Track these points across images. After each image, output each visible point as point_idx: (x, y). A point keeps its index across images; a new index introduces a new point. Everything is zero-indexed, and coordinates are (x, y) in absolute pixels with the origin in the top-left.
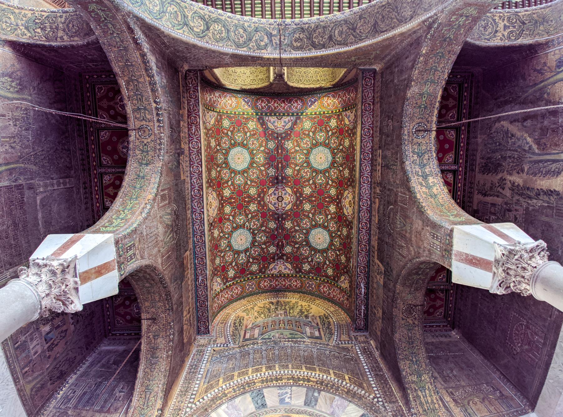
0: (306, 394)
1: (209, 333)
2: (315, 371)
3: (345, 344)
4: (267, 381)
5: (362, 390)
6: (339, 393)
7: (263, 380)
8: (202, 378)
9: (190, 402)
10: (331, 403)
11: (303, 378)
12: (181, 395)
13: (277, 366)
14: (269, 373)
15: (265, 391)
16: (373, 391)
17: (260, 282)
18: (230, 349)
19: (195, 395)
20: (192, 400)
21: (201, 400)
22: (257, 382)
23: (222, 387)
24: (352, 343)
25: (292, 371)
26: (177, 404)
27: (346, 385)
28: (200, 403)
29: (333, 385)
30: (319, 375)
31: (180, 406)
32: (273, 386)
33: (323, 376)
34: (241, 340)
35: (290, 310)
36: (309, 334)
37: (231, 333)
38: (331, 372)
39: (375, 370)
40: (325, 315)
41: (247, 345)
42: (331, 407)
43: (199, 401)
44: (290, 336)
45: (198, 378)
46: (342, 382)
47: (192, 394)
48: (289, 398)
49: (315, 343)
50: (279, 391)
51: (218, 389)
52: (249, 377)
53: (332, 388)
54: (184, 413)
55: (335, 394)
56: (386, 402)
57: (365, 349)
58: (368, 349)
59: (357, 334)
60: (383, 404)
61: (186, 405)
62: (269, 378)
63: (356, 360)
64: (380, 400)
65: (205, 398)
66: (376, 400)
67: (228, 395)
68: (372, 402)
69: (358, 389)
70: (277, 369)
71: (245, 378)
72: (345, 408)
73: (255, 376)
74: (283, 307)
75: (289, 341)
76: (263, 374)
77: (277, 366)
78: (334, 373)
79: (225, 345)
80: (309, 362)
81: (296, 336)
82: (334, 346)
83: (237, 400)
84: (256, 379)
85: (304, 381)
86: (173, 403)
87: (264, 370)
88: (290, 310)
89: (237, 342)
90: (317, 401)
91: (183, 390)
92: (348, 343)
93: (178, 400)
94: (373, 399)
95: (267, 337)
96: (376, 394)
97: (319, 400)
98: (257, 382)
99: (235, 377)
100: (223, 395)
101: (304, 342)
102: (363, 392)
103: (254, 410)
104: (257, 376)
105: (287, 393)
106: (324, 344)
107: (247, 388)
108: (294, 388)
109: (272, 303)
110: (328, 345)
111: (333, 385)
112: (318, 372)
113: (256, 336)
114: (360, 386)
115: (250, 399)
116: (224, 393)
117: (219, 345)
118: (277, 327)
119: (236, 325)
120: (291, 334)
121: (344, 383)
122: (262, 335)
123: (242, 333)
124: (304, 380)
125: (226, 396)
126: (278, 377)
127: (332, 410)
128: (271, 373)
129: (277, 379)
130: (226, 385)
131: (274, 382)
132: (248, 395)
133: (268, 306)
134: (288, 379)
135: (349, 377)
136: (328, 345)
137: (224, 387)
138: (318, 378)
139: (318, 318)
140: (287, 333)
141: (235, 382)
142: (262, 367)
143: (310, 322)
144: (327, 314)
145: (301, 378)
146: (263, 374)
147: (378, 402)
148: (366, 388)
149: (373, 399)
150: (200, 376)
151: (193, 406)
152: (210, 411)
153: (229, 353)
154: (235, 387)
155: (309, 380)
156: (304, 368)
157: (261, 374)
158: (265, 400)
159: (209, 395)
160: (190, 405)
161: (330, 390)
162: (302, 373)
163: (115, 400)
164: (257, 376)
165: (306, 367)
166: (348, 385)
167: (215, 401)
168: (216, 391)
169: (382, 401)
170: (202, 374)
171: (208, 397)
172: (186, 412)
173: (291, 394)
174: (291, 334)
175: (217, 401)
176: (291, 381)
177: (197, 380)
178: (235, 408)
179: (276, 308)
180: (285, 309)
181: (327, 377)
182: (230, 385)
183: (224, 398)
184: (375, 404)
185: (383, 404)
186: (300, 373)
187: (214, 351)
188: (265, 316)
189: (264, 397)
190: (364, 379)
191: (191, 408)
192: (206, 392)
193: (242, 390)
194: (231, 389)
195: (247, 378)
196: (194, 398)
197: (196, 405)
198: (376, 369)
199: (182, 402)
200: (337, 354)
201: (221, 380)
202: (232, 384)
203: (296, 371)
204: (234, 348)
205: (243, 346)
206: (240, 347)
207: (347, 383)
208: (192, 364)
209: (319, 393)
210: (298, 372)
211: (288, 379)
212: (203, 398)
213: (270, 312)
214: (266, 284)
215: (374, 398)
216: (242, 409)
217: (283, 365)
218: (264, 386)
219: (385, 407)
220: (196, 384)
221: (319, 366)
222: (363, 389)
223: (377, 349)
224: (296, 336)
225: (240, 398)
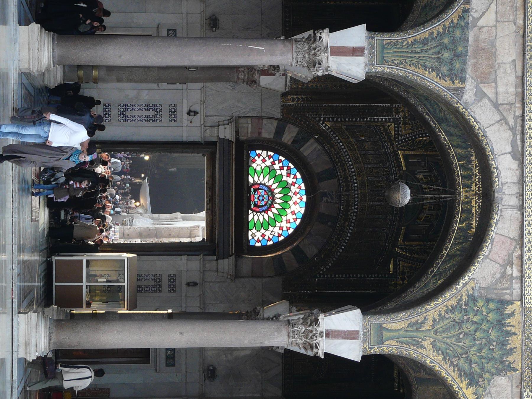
9: (324, 118)
15: (335, 180)
18: (391, 141)
21: (327, 127)
22: (345, 173)
45: (352, 119)
47: (333, 119)
50: (334, 192)
60: (317, 278)
64: (322, 276)
65: (330, 130)
66: (321, 272)
83: (327, 158)
98: (345, 173)
102: (330, 265)
105: (332, 199)
111: (339, 241)
115: (327, 167)
145: (349, 213)
147: (320, 274)
151: (321, 122)
159: (332, 133)
169: (320, 277)
171: (330, 132)
187: (389, 126)
189: (329, 179)
191: (320, 120)
197: (322, 124)
202: (344, 150)
204: (392, 145)
220: (345, 119)
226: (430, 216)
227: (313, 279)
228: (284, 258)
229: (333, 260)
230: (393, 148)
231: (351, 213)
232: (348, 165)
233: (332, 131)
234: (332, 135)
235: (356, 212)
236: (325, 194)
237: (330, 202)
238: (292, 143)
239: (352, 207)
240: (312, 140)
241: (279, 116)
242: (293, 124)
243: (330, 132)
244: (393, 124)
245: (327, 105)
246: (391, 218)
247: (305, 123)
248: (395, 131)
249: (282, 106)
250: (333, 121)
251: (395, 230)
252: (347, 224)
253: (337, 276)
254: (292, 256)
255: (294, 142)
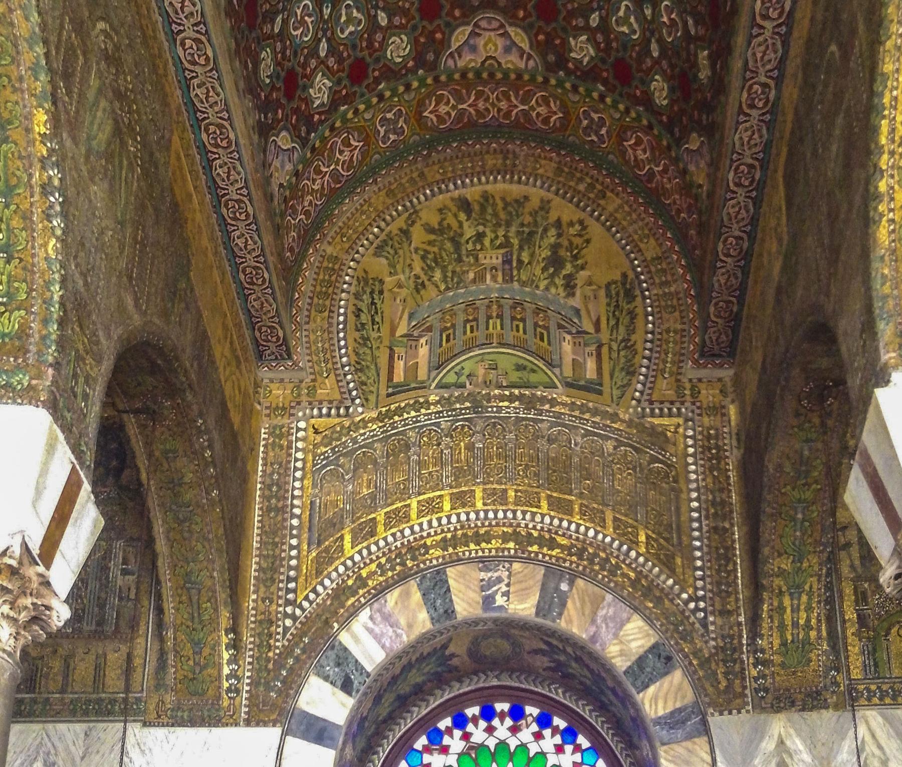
0: (543, 585)
1: (290, 357)
2: (570, 513)
3: (661, 416)
4: (455, 542)
5: (669, 577)
6: (616, 583)
7: (444, 540)
8: (300, 527)
9: (288, 603)
10: (594, 613)
11: (541, 537)
12: (264, 581)
13: (479, 494)
14: (458, 515)
15: (451, 572)
16: (691, 580)
17: (421, 105)
19: (295, 579)
20: (291, 596)
21: (312, 596)
22: (432, 547)
23: (351, 558)
24: (679, 414)
25: (514, 512)
26: (262, 607)
27: (636, 559)
28: (311, 603)
29: (607, 560)
30: (578, 525)
31: (270, 613)
32: (470, 560)
33: (587, 529)
34: (383, 392)
35: (521, 248)
36: (568, 372)
37: (354, 358)
38: (609, 516)
39: (716, 514)
40: (625, 276)
41: (399, 411)
42: (593, 621)
43: (306, 598)
44: (514, 376)
45: (292, 527)
46: (629, 549)
47: (289, 579)
48: (503, 595)
49: (583, 409)
50: (483, 575)
51: (344, 564)
52: (411, 528)
53: (603, 568)
54: (280, 630)
55: (606, 587)
56: (713, 613)
57: (709, 437)
58: (717, 437)
59: (703, 373)
60: (705, 617)
61: (281, 609)
62: (460, 532)
63: (676, 481)
64: (702, 605)
65: (320, 589)
66: (692, 605)
67: (370, 583)
68: (683, 612)
69: (661, 572)
70: (479, 505)
71: (402, 532)
72: (622, 625)
73: (425, 526)
74: (501, 232)
75: (511, 399)
76: (444, 521)
77: (479, 494)
78: (615, 519)
79: (342, 411)
80: (557, 476)
81: (534, 378)
82: (630, 424)
83: (392, 598)
84: (429, 535)
85: (541, 547)
86: (252, 604)
87: (447, 506)
88: (521, 248)
89: (373, 398)
90: (563, 605)
91: (265, 565)
92: (670, 415)
93: (261, 594)
94: (686, 603)
95: (451, 378)
96: (696, 589)
97: (570, 604)
98: (432, 547)
99: (380, 528)
100: (358, 583)
101: (553, 402)
103: (429, 626)
104: (430, 522)
105: (499, 580)
106: (604, 415)
107: (409, 563)
108: (516, 566)
109: (465, 205)
110: (615, 417)
111: (607, 560)
112: (577, 518)
113: (422, 374)
114: (668, 565)
115: (417, 596)
116: (360, 577)
117: (324, 411)
118: (480, 335)
119: (364, 318)
120: (520, 368)
121: (633, 554)
122: (439, 367)
123: (383, 361)
124: (540, 541)
125: (365, 585)
126: (482, 531)
127: (593, 629)
128: (463, 517)
129: (478, 539)
130: (360, 552)
131: (472, 546)
132: (413, 585)
133: (455, 225)
134: (505, 538)
135: (648, 537)
136: (615, 417)
137: (357, 558)
138: (574, 535)
139: (602, 293)
140: (507, 358)
141: (382, 543)
142: (441, 496)
143: (577, 312)
144: (631, 275)
145: (535, 534)
146: (444, 521)
147: (697, 609)
148: (679, 570)
149: (686, 603)
150: (295, 522)
151: (298, 612)
152: (336, 625)
153: (354, 440)
154: (383, 560)
155: (552, 544)
156: (544, 504)
157: (439, 520)
158: (451, 601)
159: (327, 582)
160: (289, 610)
161: (598, 573)
162: (538, 518)
163: (121, 599)
164: (430, 522)
165: (549, 497)
166: (641, 559)
167: (343, 598)
168: (341, 569)
169: (704, 610)
170: (299, 517)
171: (325, 588)
172: (286, 629)
173: (508, 585)
174: (520, 368)
175: (348, 599)
176: (511, 545)
177: (292, 537)
178: (387, 618)
179: (480, 236)
180: (507, 244)
181: (597, 532)
182: (370, 553)
183: (361, 592)
184: (688, 618)
185: (705, 617)
186: (533, 520)
188: (445, 279)
189: (448, 590)
190: (680, 543)
191: (294, 618)
192: (319, 573)
193: (398, 568)
194: (373, 567)
195: (407, 532)
196: (294, 591)
197: (303, 610)
198: (717, 509)
199: (271, 602)
200: (632, 455)
201: (348, 538)
202: (374, 548)
203: (524, 513)
205: (389, 415)
206: (380, 418)
207: (639, 555)
208: (268, 481)
209: (571, 583)
210: (528, 516)
211: (505, 538)
212: (314, 591)
213: (459, 260)
214: (443, 109)
215: (690, 599)
216: (403, 622)
217: (494, 492)
218: (447, 559)
219: (705, 625)
220: (292, 547)
221: (581, 495)
222: (672, 572)
223: (738, 440)
224: (534, 378)
225: (396, 593)
226: (539, 330)
227: (712, 628)
228: (661, 713)
229: (658, 576)
230: (373, 420)
231: (534, 528)
232: (411, 538)
233: (322, 583)
234: (332, 582)
235: (534, 514)
236: (488, 601)
237: (508, 585)
238: (349, 693)
239: (519, 525)
240: (344, 638)
241: (277, 731)
242: (298, 692)
243: (325, 588)
244: (313, 421)
245: (254, 597)
246: (545, 425)
247: (297, 659)
248: (329, 415)
249: (248, 723)
250: (295, 579)
251: (577, 413)
252: (563, 541)
253: (699, 563)
254: (652, 689)
255: (347, 687)
